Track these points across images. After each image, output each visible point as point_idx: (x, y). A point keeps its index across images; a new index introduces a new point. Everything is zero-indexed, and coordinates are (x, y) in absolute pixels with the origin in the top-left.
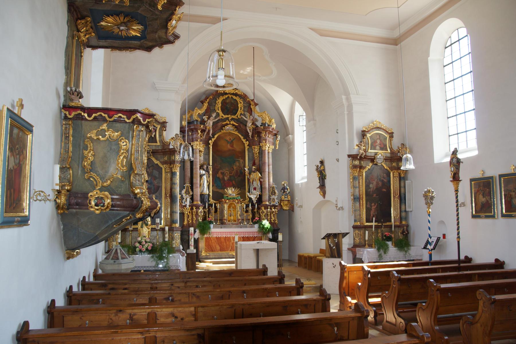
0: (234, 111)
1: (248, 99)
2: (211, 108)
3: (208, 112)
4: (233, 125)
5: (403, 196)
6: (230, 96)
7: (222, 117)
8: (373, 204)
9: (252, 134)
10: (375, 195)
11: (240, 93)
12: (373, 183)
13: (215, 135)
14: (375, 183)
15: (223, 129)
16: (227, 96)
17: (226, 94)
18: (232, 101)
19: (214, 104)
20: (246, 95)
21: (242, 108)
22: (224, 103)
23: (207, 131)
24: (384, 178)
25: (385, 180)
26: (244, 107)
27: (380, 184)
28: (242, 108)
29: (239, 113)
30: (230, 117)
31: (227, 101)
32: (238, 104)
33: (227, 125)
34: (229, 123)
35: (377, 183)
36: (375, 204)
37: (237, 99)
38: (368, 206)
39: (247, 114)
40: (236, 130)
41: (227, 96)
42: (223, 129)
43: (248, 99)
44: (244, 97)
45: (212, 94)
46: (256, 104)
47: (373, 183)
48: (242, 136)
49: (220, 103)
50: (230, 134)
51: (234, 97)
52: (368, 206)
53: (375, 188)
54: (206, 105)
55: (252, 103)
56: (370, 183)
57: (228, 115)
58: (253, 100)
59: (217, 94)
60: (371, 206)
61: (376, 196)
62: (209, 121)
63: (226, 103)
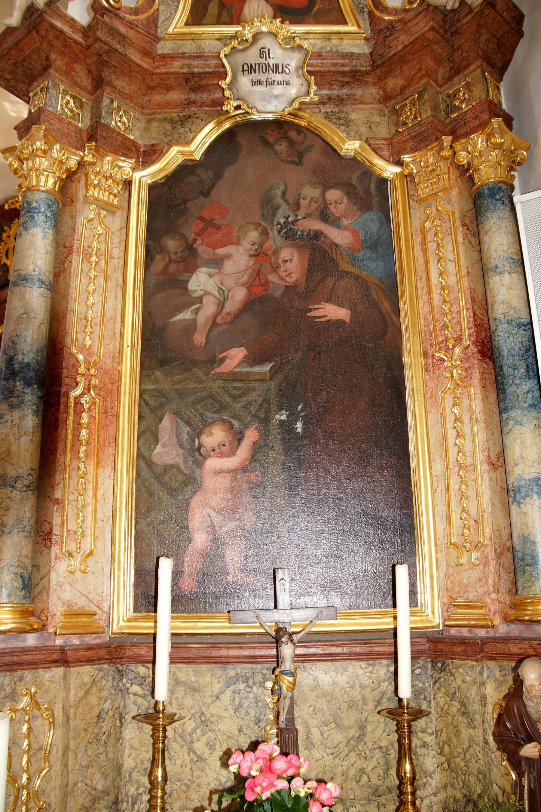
5: (508, 342)
8: (215, 436)
10: (237, 354)
12: (217, 263)
14: (238, 259)
24: (325, 216)
25: (339, 237)
27: (292, 264)
35: (260, 254)
36: (238, 437)
38: (166, 453)
47: (217, 263)
52: (166, 453)
53: (239, 295)
56: (190, 260)
60: (197, 454)
61: (253, 360)
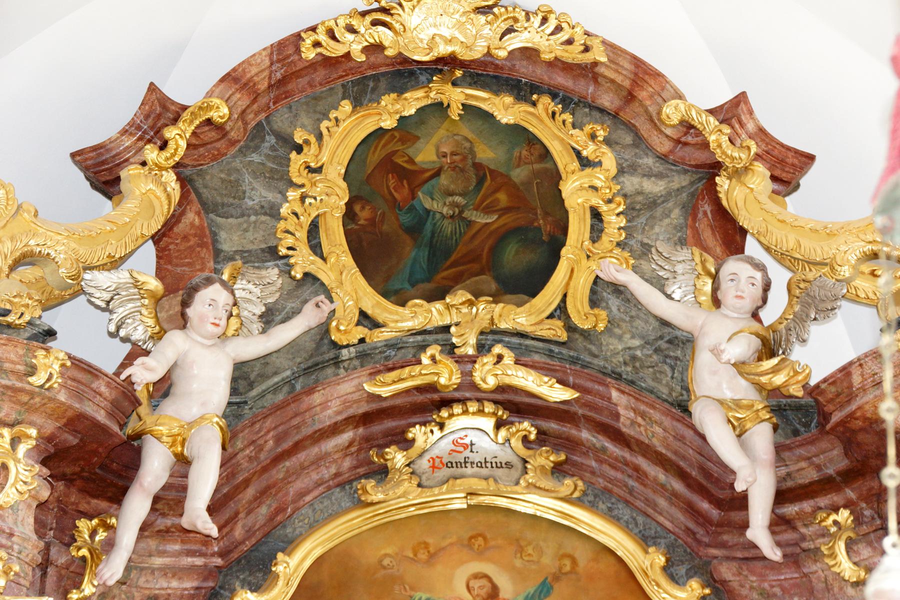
0: (514, 257)
1: (672, 112)
2: (229, 242)
3: (184, 259)
4: (513, 405)
6: (456, 96)
7: (365, 319)
9: (782, 496)
11: (573, 55)
13: (289, 545)
15: (382, 472)
16: (413, 102)
17: (405, 73)
18: (486, 154)
19: (258, 193)
20: (642, 72)
21: (614, 222)
22: (380, 171)
23: (155, 468)
26: (638, 209)
28: (614, 222)
29: (575, 270)
30: (464, 313)
31: (425, 155)
32: (556, 177)
33: (431, 403)
34: (447, 376)
37: (540, 118)
39: (685, 266)
40: (559, 470)
41: (413, 102)
42: (382, 472)
43: (672, 112)
44: (610, 90)
45: (233, 79)
46: (788, 168)
48: (646, 540)
49: (336, 171)
50: (488, 528)
51: (505, 110)
54: (151, 190)
55: (717, 137)
57: (437, 295)
58: (732, 112)
59: (292, 81)
62: (176, 343)
63: (413, 178)
